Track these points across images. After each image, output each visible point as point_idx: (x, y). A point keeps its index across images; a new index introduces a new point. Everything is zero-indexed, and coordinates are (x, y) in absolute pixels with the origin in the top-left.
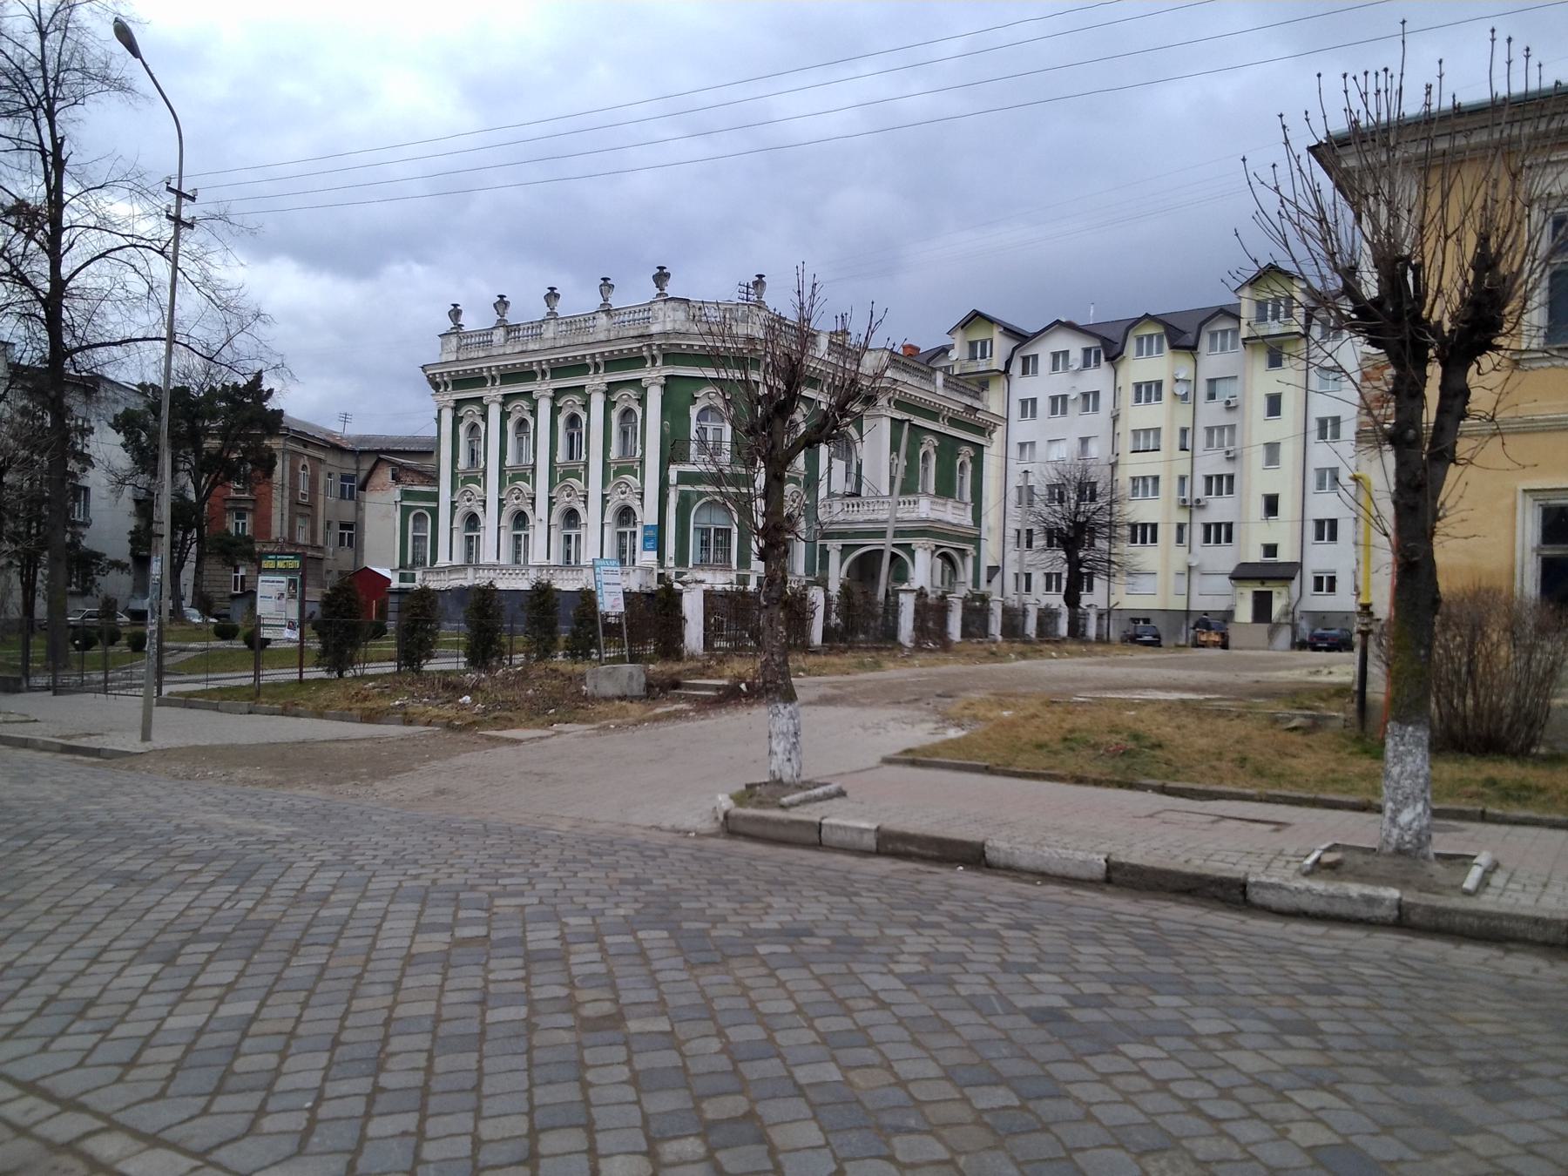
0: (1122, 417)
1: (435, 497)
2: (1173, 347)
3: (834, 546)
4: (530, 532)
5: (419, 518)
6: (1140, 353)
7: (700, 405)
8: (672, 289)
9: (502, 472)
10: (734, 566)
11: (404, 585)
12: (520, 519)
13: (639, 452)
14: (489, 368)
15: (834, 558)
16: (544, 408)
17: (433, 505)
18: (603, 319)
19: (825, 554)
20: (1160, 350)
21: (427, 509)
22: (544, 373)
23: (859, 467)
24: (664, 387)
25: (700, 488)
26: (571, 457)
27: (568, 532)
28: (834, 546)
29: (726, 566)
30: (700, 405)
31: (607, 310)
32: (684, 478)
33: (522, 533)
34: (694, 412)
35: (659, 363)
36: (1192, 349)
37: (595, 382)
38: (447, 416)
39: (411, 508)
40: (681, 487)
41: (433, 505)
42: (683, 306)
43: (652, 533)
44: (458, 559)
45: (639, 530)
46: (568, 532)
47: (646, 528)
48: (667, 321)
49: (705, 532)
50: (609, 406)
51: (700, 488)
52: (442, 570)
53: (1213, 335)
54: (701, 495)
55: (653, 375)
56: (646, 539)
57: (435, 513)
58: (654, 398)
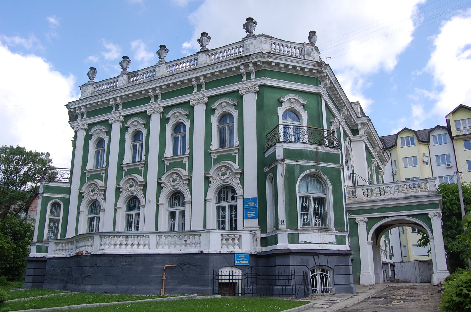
0: (397, 174)
2: (420, 141)
3: (361, 220)
4: (142, 212)
5: (56, 206)
6: (403, 145)
7: (285, 106)
8: (257, 31)
9: (120, 169)
12: (133, 202)
14: (115, 99)
15: (362, 228)
17: (66, 196)
19: (354, 225)
20: (413, 143)
21: (61, 199)
22: (156, 97)
23: (353, 171)
24: (257, 93)
25: (300, 163)
27: (173, 209)
28: (361, 220)
29: (328, 230)
30: (285, 106)
31: (205, 51)
32: (289, 154)
33: (134, 212)
34: (281, 111)
35: (253, 76)
36: (427, 142)
37: (197, 98)
38: (82, 135)
39: (49, 199)
40: (288, 162)
41: (66, 196)
42: (268, 41)
45: (239, 203)
46: (173, 209)
47: (246, 201)
49: (305, 199)
50: (210, 112)
51: (300, 163)
52: (71, 241)
53: (434, 136)
54: (303, 168)
55: (248, 88)
56: (245, 210)
57: (67, 202)
58: (250, 103)
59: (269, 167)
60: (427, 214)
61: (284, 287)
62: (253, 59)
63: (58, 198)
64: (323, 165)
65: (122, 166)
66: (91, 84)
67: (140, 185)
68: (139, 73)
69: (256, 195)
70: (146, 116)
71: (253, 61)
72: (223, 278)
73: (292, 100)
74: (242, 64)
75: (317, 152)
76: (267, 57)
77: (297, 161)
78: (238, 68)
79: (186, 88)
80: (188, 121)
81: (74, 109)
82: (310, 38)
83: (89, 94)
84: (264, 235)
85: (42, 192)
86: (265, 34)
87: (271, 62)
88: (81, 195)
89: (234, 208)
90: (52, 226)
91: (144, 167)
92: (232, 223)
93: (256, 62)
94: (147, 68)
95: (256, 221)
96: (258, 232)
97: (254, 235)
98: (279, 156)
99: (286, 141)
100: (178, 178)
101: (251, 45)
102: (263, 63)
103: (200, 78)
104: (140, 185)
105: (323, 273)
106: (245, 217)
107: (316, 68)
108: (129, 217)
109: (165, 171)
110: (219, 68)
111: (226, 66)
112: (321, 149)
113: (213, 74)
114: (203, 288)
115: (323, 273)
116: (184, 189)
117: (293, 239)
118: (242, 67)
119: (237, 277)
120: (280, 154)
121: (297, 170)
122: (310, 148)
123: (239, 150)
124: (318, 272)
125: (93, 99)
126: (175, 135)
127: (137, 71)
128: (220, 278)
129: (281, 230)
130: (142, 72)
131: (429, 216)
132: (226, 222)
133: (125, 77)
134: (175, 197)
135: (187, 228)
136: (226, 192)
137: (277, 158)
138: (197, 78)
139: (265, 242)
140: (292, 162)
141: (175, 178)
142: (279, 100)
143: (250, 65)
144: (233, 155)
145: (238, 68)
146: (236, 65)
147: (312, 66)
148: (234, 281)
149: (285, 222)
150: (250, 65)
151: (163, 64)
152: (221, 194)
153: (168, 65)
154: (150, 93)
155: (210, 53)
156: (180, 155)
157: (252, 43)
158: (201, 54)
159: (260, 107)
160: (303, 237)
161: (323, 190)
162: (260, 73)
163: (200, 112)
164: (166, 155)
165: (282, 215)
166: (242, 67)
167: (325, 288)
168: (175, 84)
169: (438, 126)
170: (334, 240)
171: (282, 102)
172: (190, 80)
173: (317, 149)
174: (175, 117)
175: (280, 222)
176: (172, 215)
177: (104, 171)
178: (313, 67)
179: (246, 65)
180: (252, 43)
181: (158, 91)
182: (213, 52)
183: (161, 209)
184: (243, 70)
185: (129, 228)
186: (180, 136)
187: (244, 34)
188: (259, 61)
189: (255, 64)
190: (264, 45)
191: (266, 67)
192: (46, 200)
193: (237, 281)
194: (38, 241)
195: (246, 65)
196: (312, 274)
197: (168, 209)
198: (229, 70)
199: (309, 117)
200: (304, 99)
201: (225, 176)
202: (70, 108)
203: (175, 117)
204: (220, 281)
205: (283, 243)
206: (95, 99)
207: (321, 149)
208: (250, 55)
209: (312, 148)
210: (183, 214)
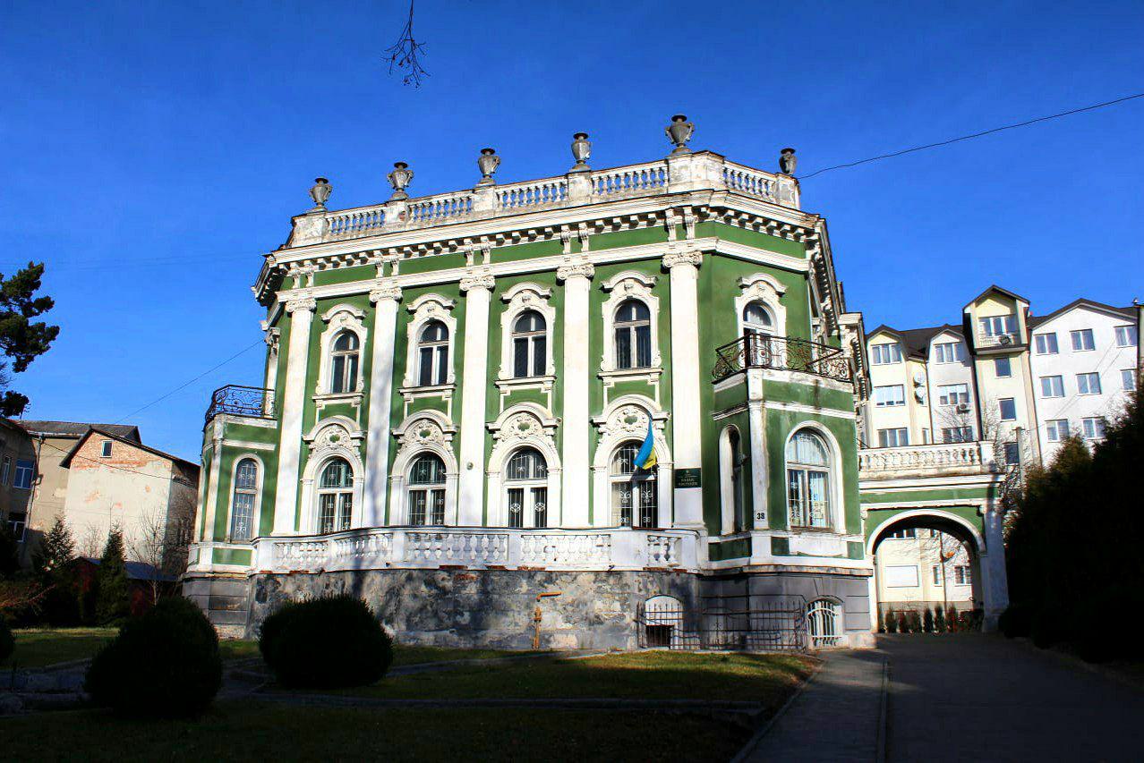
1: (275, 437)
10: (841, 526)
16: (478, 304)
21: (261, 454)
26: (521, 370)
27: (516, 484)
32: (773, 392)
34: (740, 304)
35: (691, 231)
40: (772, 405)
41: (271, 447)
44: (310, 525)
45: (664, 479)
54: (794, 417)
57: (271, 460)
58: (684, 284)
59: (725, 412)
63: (253, 451)
64: (826, 412)
65: (402, 391)
70: (458, 294)
71: (695, 203)
75: (816, 389)
77: (785, 405)
78: (661, 214)
82: (783, 163)
84: (715, 539)
85: (221, 436)
90: (240, 509)
91: (453, 396)
96: (704, 533)
97: (698, 537)
99: (766, 367)
101: (683, 171)
105: (827, 609)
107: (804, 225)
108: (417, 496)
109: (502, 409)
111: (636, 207)
112: (823, 383)
115: (827, 609)
116: (543, 443)
117: (780, 547)
119: (670, 616)
120: (756, 390)
121: (785, 421)
122: (807, 380)
124: (818, 606)
126: (520, 335)
135: (552, 520)
139: (716, 552)
140: (777, 406)
143: (688, 211)
144: (650, 383)
148: (668, 623)
149: (766, 516)
150: (688, 211)
156: (531, 377)
157: (686, 167)
159: (705, 295)
160: (796, 542)
163: (577, 294)
164: (501, 375)
166: (669, 213)
167: (831, 636)
169: (947, 326)
170: (845, 552)
173: (817, 382)
174: (520, 298)
175: (756, 516)
176: (516, 495)
183: (492, 481)
184: (673, 219)
185: (417, 518)
186: (530, 338)
189: (696, 210)
190: (710, 173)
194: (216, 539)
196: (809, 610)
197: (506, 483)
199: (789, 317)
200: (782, 282)
201: (634, 424)
202: (278, 261)
203: (520, 298)
206: (339, 248)
207: (823, 383)
209: (808, 380)
210: (541, 493)
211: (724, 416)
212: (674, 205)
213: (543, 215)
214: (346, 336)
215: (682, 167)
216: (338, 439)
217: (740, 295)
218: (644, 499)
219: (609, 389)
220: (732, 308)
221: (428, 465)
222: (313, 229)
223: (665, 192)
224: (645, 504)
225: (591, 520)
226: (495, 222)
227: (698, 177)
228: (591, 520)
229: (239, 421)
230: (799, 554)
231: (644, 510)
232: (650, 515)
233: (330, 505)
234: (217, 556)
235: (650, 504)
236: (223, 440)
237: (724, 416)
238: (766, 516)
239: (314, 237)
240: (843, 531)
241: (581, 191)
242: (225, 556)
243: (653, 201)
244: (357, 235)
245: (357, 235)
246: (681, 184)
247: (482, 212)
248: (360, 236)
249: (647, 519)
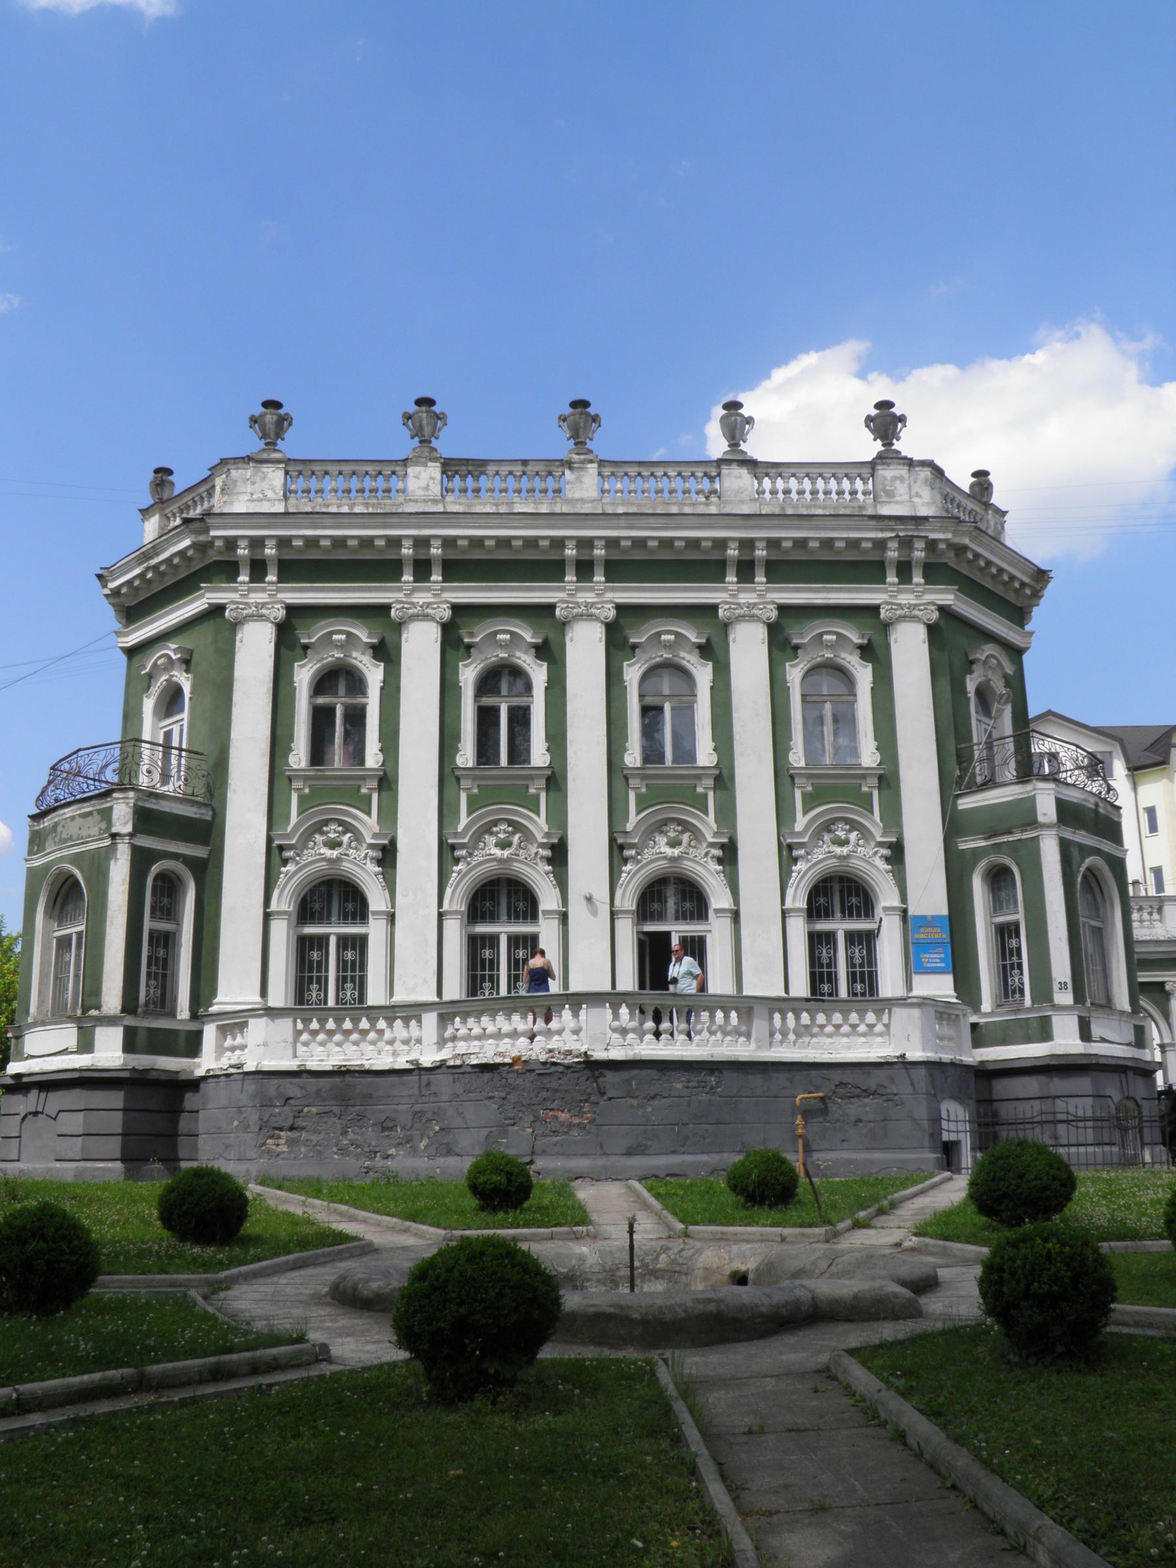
11: (143, 1061)
13: (869, 756)
17: (199, 852)
18: (738, 481)
40: (1068, 834)
41: (199, 852)
43: (945, 936)
48: (912, 499)
58: (910, 651)
59: (985, 839)
60: (1162, 984)
61: (1082, 1149)
62: (933, 531)
66: (278, 461)
67: (542, 845)
68: (491, 469)
69: (945, 911)
71: (932, 536)
72: (952, 1126)
73: (995, 662)
74: (897, 536)
76: (964, 534)
79: (703, 565)
80: (705, 666)
81: (231, 543)
83: (270, 494)
85: (128, 828)
86: (938, 462)
87: (965, 548)
88: (275, 855)
89: (865, 941)
92: (854, 981)
93: (934, 541)
94: (525, 462)
95: (949, 980)
98: (1045, 814)
100: (685, 838)
101: (898, 483)
102: (951, 545)
103: (758, 544)
104: (542, 845)
106: (912, 967)
110: (825, 529)
113: (801, 543)
114: (914, 1156)
118: (894, 545)
121: (1075, 852)
123: (881, 778)
125: (328, 521)
127: (483, 463)
128: (944, 1124)
129: (1054, 1007)
130: (504, 470)
131: (1167, 988)
132: (838, 976)
133: (434, 470)
134: (652, 893)
136: (838, 894)
137: (1041, 819)
138: (747, 544)
141: (672, 834)
142: (966, 656)
143: (919, 544)
145: (881, 545)
146: (880, 535)
147: (1023, 573)
150: (919, 544)
151: (591, 462)
152: (817, 895)
153: (607, 471)
154: (570, 552)
155: (760, 470)
157: (902, 479)
158: (734, 466)
161: (1097, 909)
162: (935, 573)
165: (1061, 966)
168: (667, 543)
171: (972, 662)
172: (721, 544)
173: (1097, 805)
175: (1056, 987)
177: (375, 784)
178: (1026, 580)
179: (906, 543)
180: (902, 479)
181: (599, 552)
182: (772, 471)
184: (892, 554)
186: (667, 707)
187: (868, 448)
188: (946, 541)
189: (931, 545)
191: (950, 559)
192: (141, 860)
193: (961, 1136)
195: (906, 543)
198: (854, 544)
202: (213, 533)
204: (945, 1137)
205: (1066, 1040)
208: (925, 519)
211: (983, 843)
212: (901, 534)
213: (664, 520)
214: (338, 678)
215: (895, 478)
216: (340, 844)
217: (971, 672)
218: (852, 958)
219: (803, 794)
220: (965, 692)
221: (500, 896)
222: (264, 485)
223: (870, 512)
224: (853, 966)
225: (787, 990)
226: (623, 522)
227: (918, 495)
228: (787, 990)
229: (151, 805)
230: (1103, 1040)
231: (854, 974)
232: (862, 981)
233: (315, 955)
234: (129, 1046)
235: (862, 965)
236: (131, 835)
237: (983, 843)
238: (1070, 985)
239: (269, 500)
240: (1127, 1007)
241: (740, 491)
242: (141, 1038)
243: (873, 523)
244: (352, 506)
245: (352, 506)
246: (897, 502)
247: (583, 501)
248: (357, 510)
249: (859, 987)
